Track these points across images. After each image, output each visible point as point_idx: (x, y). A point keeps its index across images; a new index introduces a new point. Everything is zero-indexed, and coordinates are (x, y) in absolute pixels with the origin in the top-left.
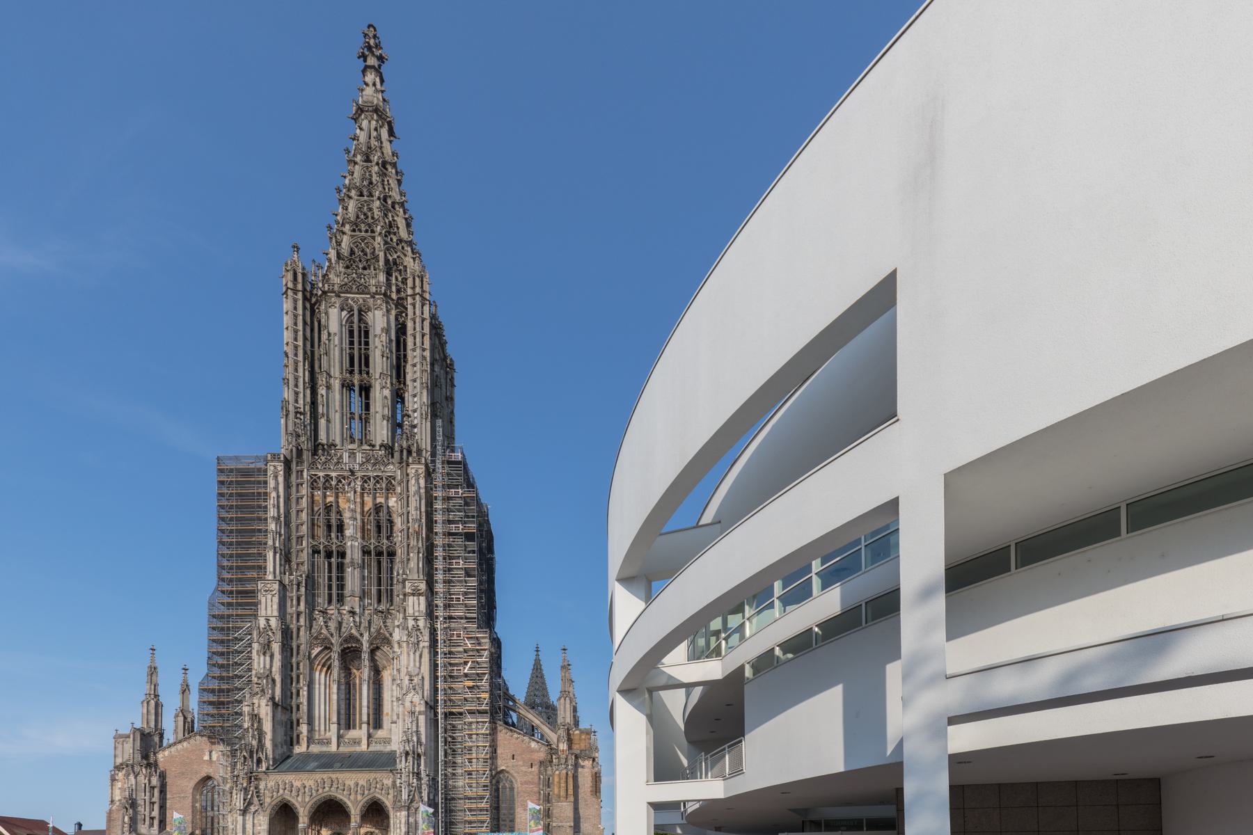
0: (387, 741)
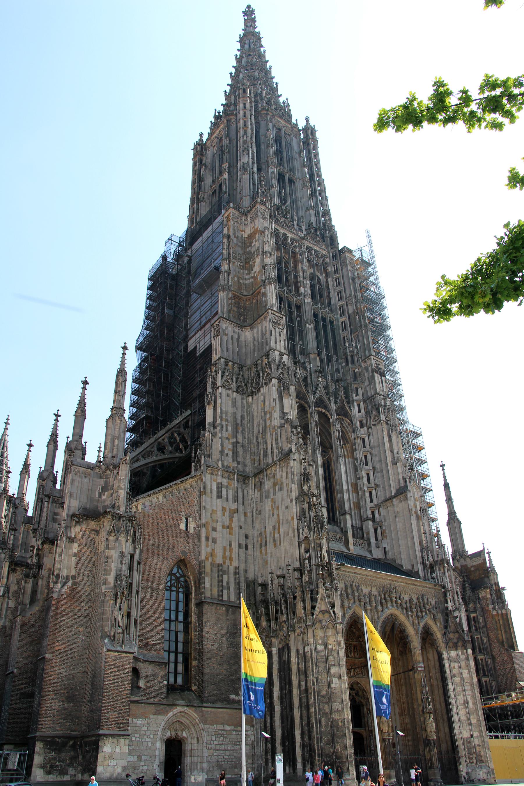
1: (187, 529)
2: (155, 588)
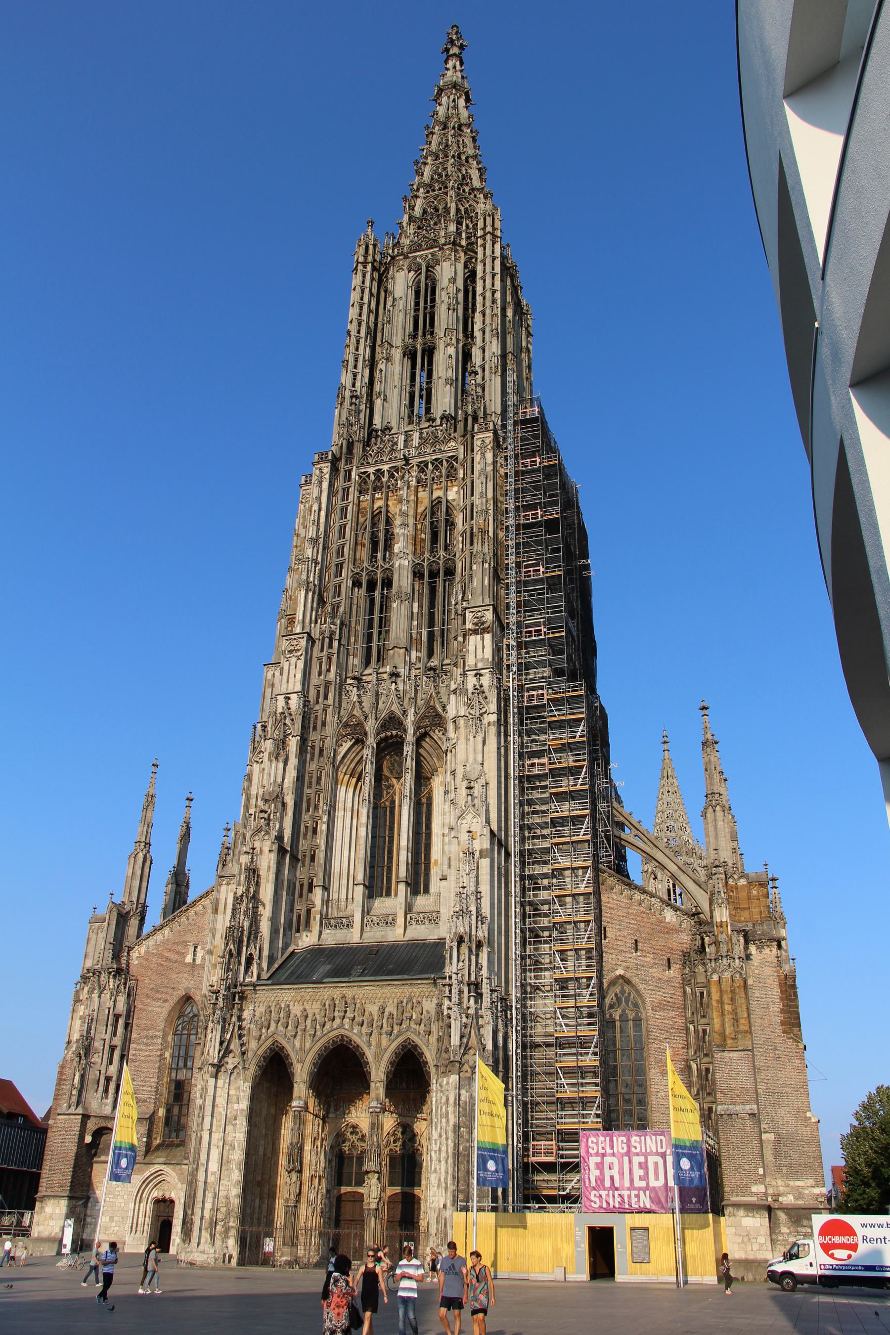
0: (433, 918)
1: (194, 960)
2: (152, 1037)
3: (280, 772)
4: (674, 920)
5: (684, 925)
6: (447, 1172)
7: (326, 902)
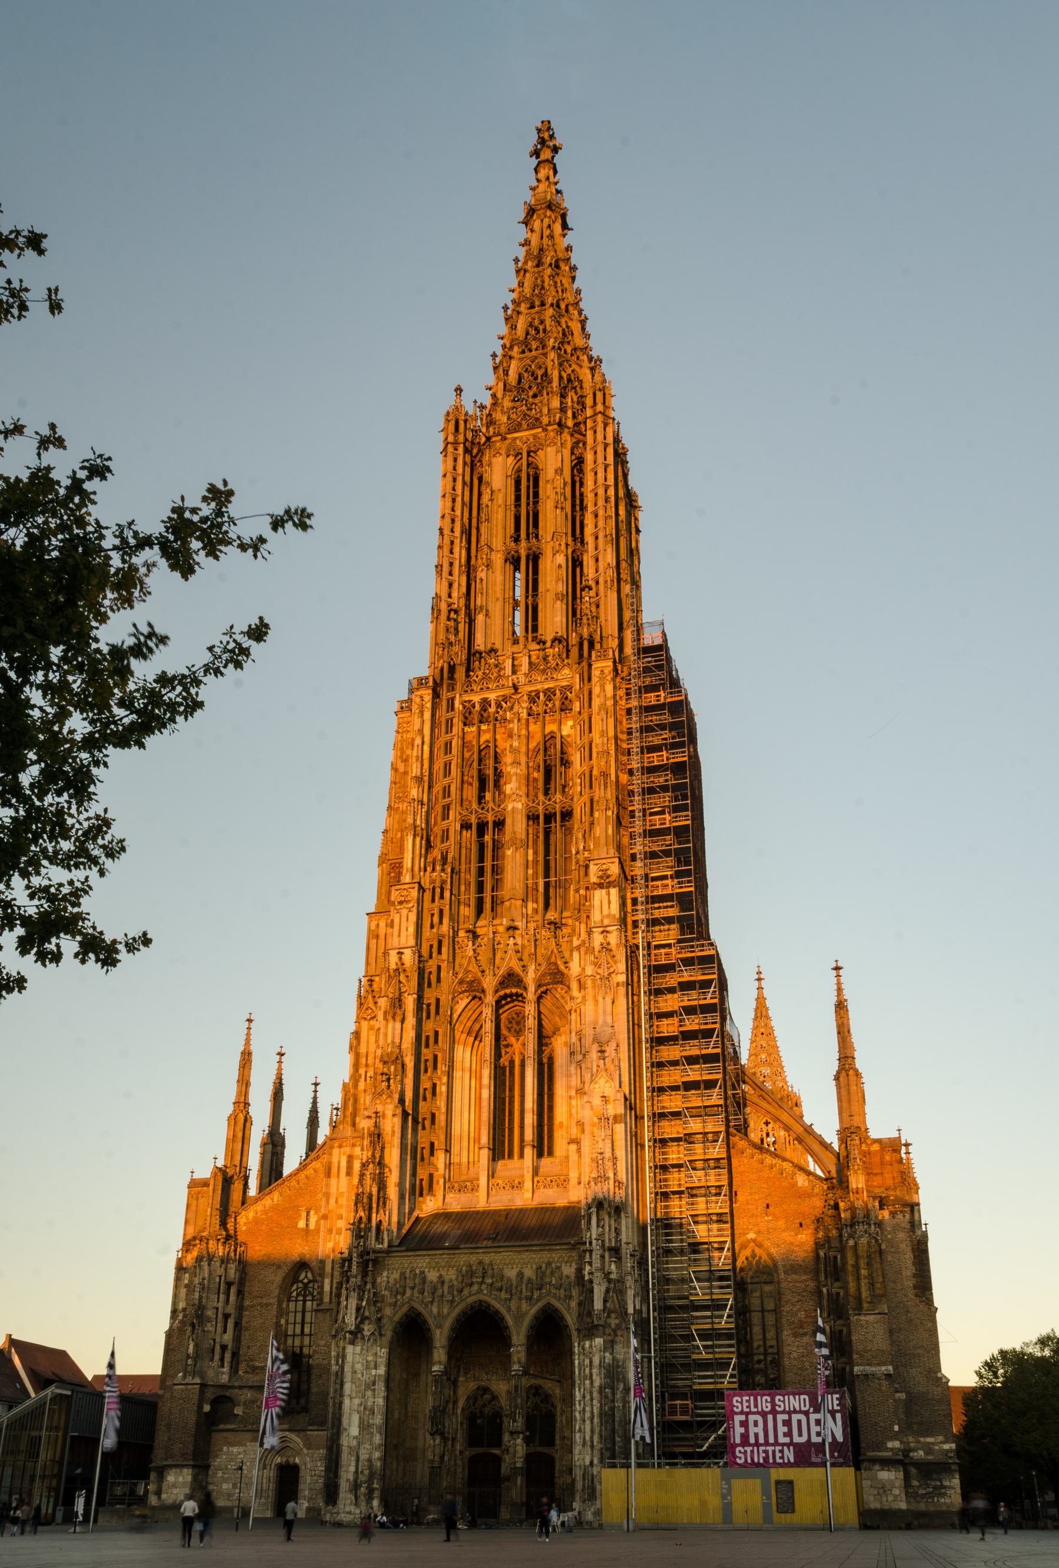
0: (563, 1182)
3: (398, 1031)
4: (806, 1184)
5: (816, 1190)
6: (592, 1431)
7: (449, 1165)
